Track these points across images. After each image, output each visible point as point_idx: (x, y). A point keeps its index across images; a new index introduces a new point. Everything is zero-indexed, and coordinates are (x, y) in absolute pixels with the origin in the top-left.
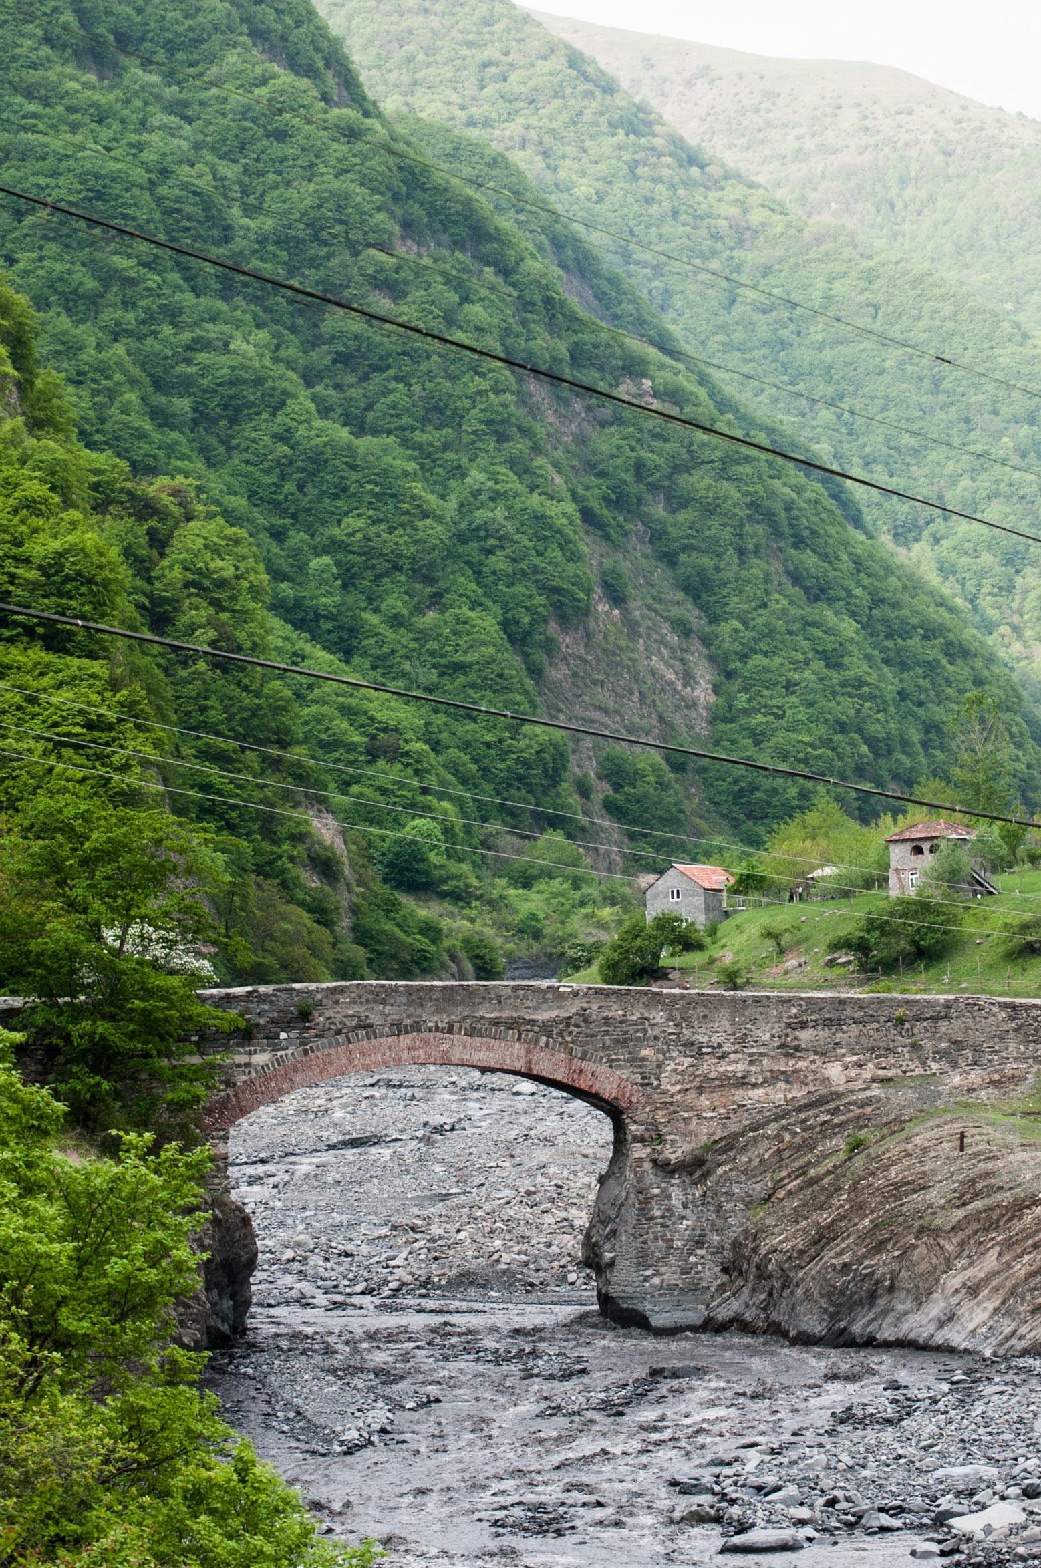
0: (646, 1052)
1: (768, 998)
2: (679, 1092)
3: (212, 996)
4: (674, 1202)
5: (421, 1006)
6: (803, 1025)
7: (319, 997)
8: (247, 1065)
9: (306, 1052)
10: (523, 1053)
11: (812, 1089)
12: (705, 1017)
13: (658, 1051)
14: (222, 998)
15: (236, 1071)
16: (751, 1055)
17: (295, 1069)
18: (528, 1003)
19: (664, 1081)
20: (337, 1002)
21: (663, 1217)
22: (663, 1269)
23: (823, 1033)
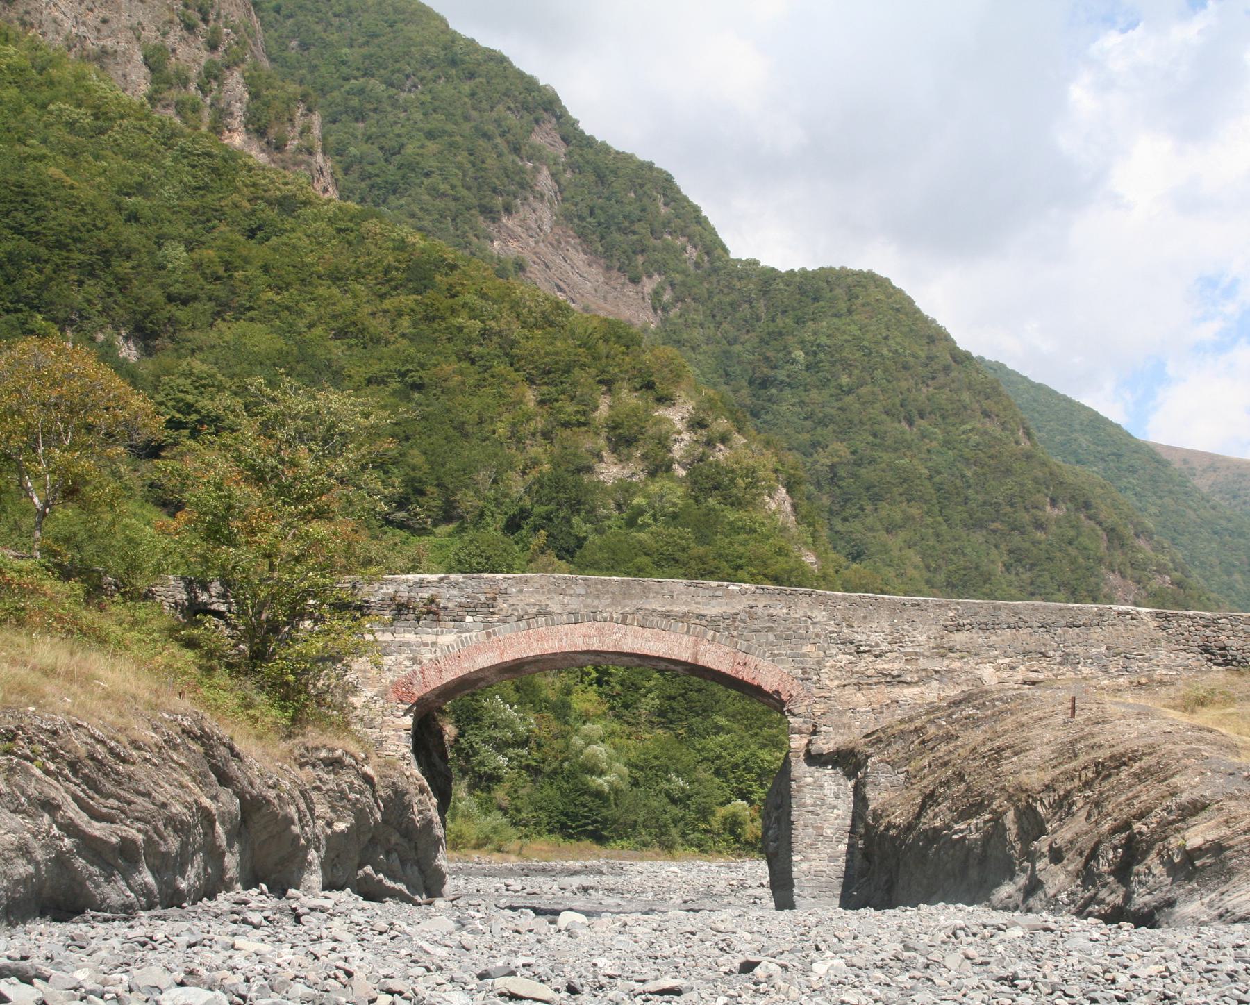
0: (807, 648)
1: (926, 602)
2: (838, 687)
3: (407, 580)
4: (826, 791)
5: (598, 597)
6: (959, 628)
7: (505, 586)
8: (434, 644)
9: (489, 635)
10: (690, 644)
11: (966, 689)
12: (865, 617)
13: (819, 649)
14: (416, 583)
15: (423, 650)
16: (906, 654)
17: (477, 649)
18: (699, 599)
19: (823, 676)
20: (521, 591)
21: (814, 805)
22: (812, 856)
23: (978, 638)
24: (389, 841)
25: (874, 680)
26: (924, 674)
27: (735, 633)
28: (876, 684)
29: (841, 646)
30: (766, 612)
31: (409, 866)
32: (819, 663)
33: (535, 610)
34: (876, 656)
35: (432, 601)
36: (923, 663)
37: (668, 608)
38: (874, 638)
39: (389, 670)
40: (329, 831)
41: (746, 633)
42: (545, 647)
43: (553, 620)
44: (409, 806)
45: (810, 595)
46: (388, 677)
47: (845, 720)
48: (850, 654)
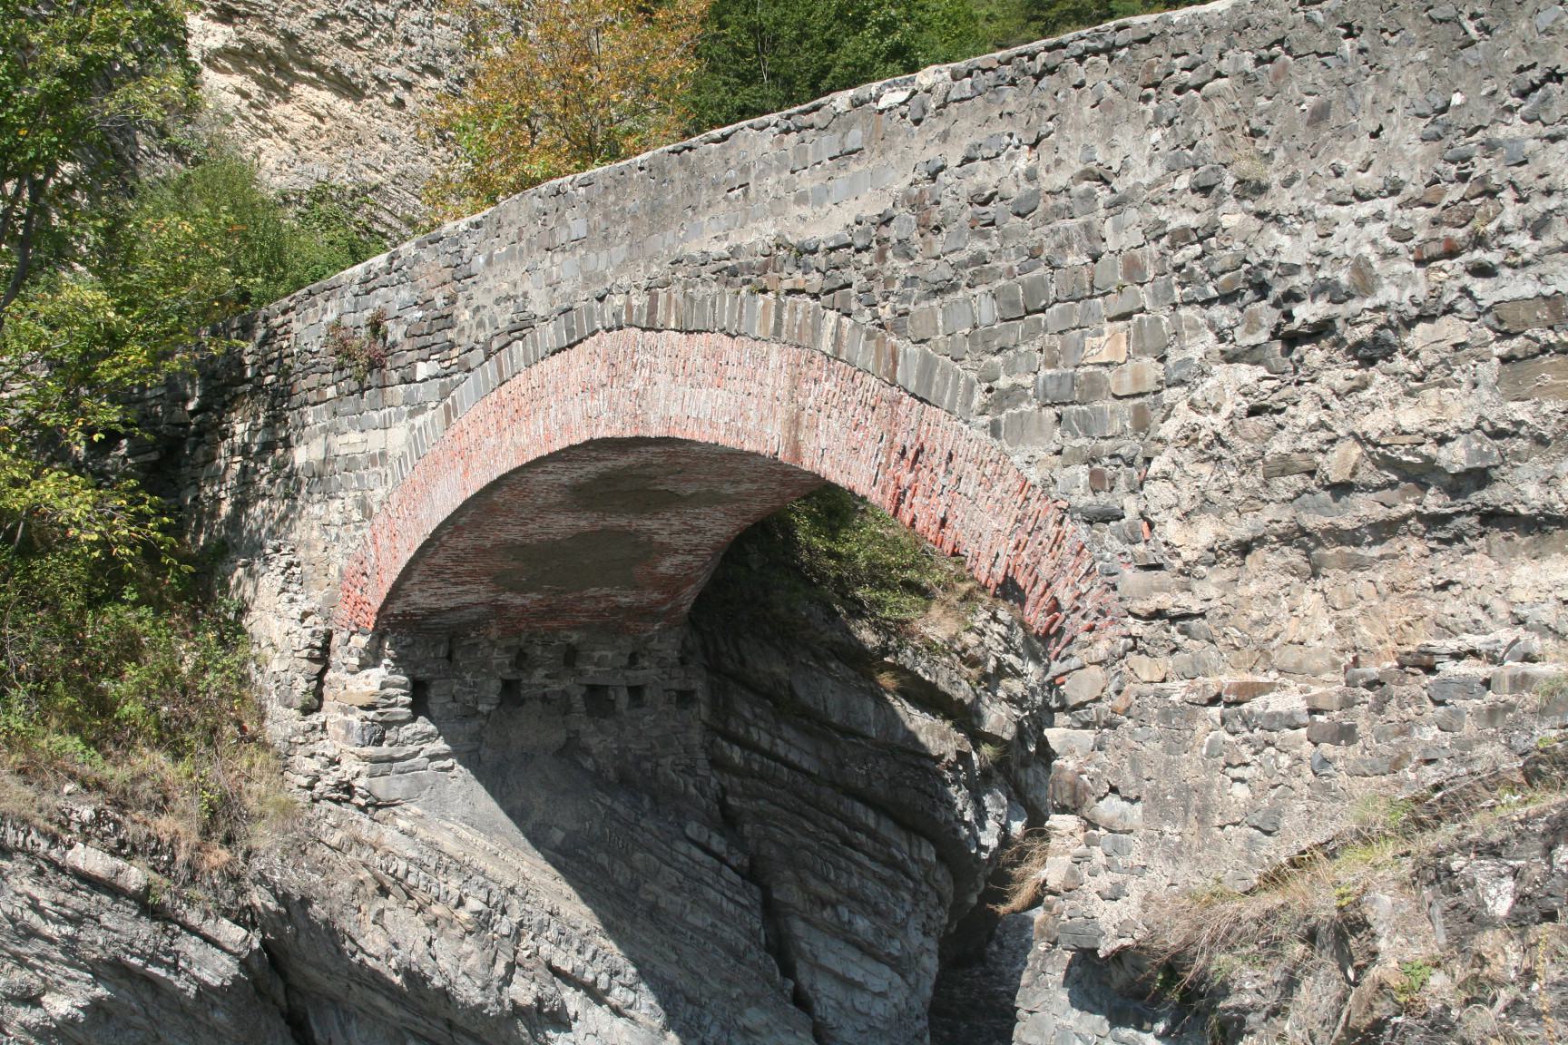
0: (1106, 345)
2: (1214, 556)
8: (383, 454)
10: (785, 382)
12: (1319, 116)
15: (370, 476)
18: (806, 181)
24: (382, 1011)
25: (1365, 508)
27: (885, 313)
28: (1385, 530)
29: (1218, 311)
30: (968, 186)
32: (1141, 423)
33: (505, 317)
34: (1371, 353)
35: (376, 326)
37: (735, 239)
38: (1357, 236)
39: (338, 537)
40: (30, 1016)
42: (525, 440)
43: (534, 341)
44: (331, 935)
45: (1110, 50)
46: (338, 561)
47: (1190, 768)
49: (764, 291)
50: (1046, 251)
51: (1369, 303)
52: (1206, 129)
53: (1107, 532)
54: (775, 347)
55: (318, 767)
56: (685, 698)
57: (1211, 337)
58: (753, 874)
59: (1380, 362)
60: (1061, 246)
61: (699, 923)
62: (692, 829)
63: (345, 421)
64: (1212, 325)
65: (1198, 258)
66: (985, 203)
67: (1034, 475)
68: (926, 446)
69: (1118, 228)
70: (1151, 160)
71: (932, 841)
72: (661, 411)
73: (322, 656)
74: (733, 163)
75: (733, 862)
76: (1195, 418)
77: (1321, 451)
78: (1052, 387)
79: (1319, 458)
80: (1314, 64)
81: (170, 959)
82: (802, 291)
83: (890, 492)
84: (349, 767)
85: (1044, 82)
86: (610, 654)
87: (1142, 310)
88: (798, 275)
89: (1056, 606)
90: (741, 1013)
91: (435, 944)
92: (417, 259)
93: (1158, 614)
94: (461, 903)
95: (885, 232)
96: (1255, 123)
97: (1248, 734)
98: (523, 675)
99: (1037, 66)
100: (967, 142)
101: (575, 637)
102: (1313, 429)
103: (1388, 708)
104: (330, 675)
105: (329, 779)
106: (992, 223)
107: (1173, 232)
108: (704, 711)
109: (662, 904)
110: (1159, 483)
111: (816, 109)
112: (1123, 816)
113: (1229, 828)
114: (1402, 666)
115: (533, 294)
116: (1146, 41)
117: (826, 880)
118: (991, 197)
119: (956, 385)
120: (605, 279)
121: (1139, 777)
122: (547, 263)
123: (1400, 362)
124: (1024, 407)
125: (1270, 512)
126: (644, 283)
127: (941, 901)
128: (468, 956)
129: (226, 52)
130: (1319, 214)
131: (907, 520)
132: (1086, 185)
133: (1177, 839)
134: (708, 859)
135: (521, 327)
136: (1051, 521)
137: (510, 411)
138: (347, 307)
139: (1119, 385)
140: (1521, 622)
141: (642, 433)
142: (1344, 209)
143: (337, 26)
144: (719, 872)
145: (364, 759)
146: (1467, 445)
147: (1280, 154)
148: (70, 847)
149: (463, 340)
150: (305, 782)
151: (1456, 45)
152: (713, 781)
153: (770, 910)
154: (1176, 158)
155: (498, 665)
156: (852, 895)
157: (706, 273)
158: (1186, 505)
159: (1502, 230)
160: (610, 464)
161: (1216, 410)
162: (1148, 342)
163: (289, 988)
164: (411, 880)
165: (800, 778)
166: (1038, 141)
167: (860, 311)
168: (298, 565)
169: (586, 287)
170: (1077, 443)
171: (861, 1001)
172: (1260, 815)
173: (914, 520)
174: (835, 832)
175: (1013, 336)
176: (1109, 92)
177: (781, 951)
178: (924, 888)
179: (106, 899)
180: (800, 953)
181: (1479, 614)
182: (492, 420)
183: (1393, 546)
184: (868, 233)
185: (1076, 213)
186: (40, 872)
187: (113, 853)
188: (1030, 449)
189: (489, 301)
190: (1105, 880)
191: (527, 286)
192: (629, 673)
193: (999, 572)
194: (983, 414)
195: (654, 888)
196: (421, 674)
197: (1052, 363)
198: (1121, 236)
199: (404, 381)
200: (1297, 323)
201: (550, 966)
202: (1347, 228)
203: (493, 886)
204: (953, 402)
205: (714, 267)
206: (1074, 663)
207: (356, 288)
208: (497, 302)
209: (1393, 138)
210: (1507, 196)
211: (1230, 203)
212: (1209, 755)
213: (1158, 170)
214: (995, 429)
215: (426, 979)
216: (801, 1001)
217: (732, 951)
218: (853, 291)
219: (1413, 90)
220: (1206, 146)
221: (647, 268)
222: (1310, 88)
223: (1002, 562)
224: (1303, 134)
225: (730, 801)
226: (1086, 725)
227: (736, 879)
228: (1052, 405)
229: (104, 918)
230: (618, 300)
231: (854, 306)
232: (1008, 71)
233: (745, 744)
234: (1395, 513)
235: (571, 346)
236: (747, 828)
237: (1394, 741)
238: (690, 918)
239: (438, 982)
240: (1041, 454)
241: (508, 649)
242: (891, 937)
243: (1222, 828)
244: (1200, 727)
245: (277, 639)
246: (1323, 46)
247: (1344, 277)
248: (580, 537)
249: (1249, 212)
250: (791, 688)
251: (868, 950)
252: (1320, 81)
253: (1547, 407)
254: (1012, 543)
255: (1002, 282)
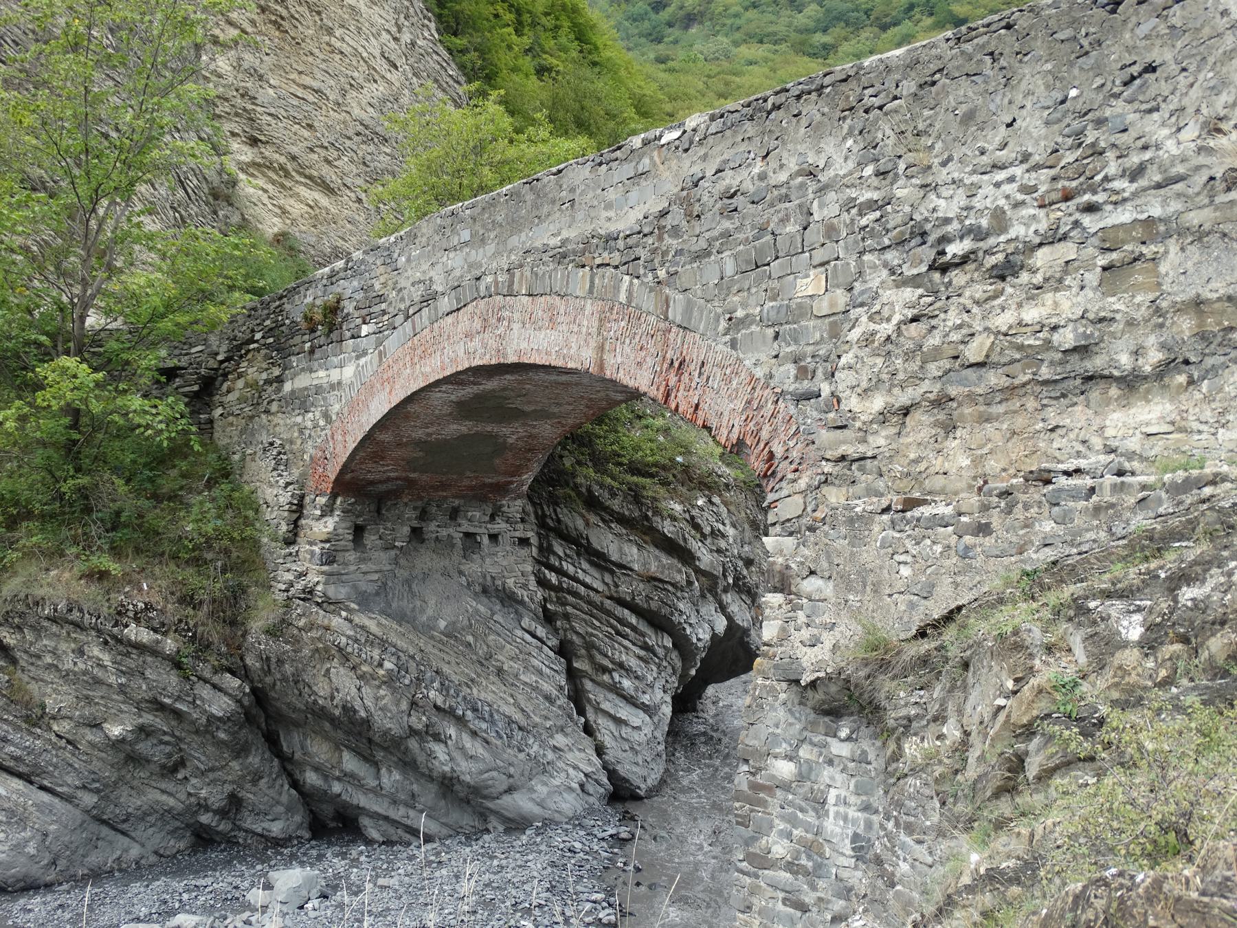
0: (809, 285)
2: (883, 418)
8: (339, 383)
12: (969, 117)
15: (332, 397)
25: (994, 378)
26: (1186, 325)
27: (662, 273)
29: (892, 257)
30: (721, 186)
31: (384, 771)
32: (835, 332)
33: (417, 293)
34: (1003, 273)
36: (1180, 270)
37: (565, 234)
41: (687, 270)
42: (428, 369)
43: (436, 309)
48: (914, 281)
49: (583, 266)
50: (772, 225)
51: (1002, 238)
52: (885, 131)
53: (809, 408)
54: (589, 301)
55: (292, 578)
56: (524, 542)
57: (885, 273)
58: (564, 651)
59: (1008, 279)
60: (782, 220)
61: (528, 680)
62: (526, 622)
63: (316, 364)
64: (885, 264)
65: (877, 220)
66: (732, 197)
67: (759, 373)
68: (687, 359)
69: (821, 206)
70: (846, 159)
71: (670, 635)
72: (515, 347)
73: (298, 509)
74: (564, 187)
75: (549, 644)
76: (872, 326)
77: (962, 342)
78: (773, 314)
79: (961, 347)
80: (964, 81)
81: (190, 699)
82: (608, 265)
83: (662, 389)
84: (313, 578)
85: (772, 116)
86: (478, 514)
87: (837, 259)
88: (605, 254)
89: (771, 455)
90: (552, 736)
91: (363, 690)
92: (363, 261)
93: (843, 458)
94: (380, 665)
95: (663, 222)
96: (921, 127)
97: (910, 532)
98: (424, 524)
99: (769, 105)
100: (718, 160)
101: (457, 502)
102: (960, 327)
103: (1015, 510)
104: (303, 522)
105: (299, 586)
106: (736, 210)
107: (861, 204)
108: (535, 551)
109: (505, 668)
110: (846, 371)
111: (619, 148)
112: (820, 590)
113: (895, 596)
114: (1027, 481)
115: (435, 278)
116: (845, 80)
117: (606, 656)
118: (735, 193)
119: (708, 318)
120: (481, 266)
121: (830, 563)
122: (445, 258)
123: (1024, 277)
124: (754, 328)
125: (925, 386)
126: (506, 267)
127: (674, 672)
128: (383, 697)
129: (254, 164)
130: (967, 182)
131: (673, 406)
132: (800, 179)
133: (858, 604)
134: (534, 641)
135: (429, 299)
136: (770, 402)
137: (419, 352)
138: (320, 294)
139: (819, 309)
140: (1113, 451)
141: (502, 361)
142: (985, 177)
143: (323, 153)
144: (541, 650)
145: (323, 573)
146: (1075, 330)
147: (939, 145)
148: (127, 626)
149: (391, 310)
150: (283, 587)
151: (1073, 56)
152: (539, 594)
153: (572, 675)
154: (863, 156)
155: (409, 519)
156: (621, 665)
157: (546, 258)
158: (864, 385)
159: (1106, 179)
160: (481, 387)
161: (888, 320)
162: (841, 279)
163: (268, 717)
164: (349, 650)
165: (591, 594)
166: (768, 154)
167: (645, 275)
168: (285, 454)
169: (469, 272)
170: (789, 350)
171: (625, 731)
172: (919, 586)
173: (677, 407)
174: (612, 627)
175: (747, 282)
176: (818, 117)
177: (578, 699)
178: (665, 663)
179: (149, 659)
180: (589, 700)
181: (1081, 448)
182: (408, 358)
183: (1016, 404)
184: (651, 223)
185: (793, 198)
186: (106, 643)
187: (155, 630)
188: (757, 356)
189: (408, 285)
190: (805, 634)
191: (432, 273)
192: (489, 526)
193: (734, 437)
194: (725, 334)
195: (500, 658)
196: (360, 521)
197: (774, 299)
198: (826, 210)
199: (353, 337)
200: (949, 256)
201: (435, 706)
202: (988, 190)
203: (401, 654)
204: (706, 329)
205: (551, 254)
206: (784, 493)
207: (324, 281)
208: (413, 284)
209: (1024, 124)
210: (1111, 155)
211: (900, 183)
212: (883, 547)
213: (851, 165)
214: (733, 344)
215: (355, 711)
216: (588, 730)
217: (548, 698)
218: (641, 262)
219: (1041, 90)
220: (886, 145)
221: (508, 257)
222: (962, 99)
223: (736, 430)
224: (955, 129)
225: (549, 606)
226: (791, 534)
227: (551, 654)
228: (773, 325)
229: (148, 673)
230: (489, 279)
231: (642, 271)
232: (749, 111)
233: (560, 572)
234: (1017, 382)
235: (458, 309)
236: (559, 623)
237: (1021, 532)
238: (522, 677)
239: (363, 714)
240: (763, 357)
241: (415, 508)
242: (644, 692)
243: (890, 596)
244: (876, 528)
245: (269, 500)
246: (971, 68)
247: (984, 222)
248: (463, 438)
249: (915, 186)
250: (587, 539)
251: (631, 701)
252: (970, 94)
253: (1138, 299)
254: (744, 417)
255: (742, 247)
